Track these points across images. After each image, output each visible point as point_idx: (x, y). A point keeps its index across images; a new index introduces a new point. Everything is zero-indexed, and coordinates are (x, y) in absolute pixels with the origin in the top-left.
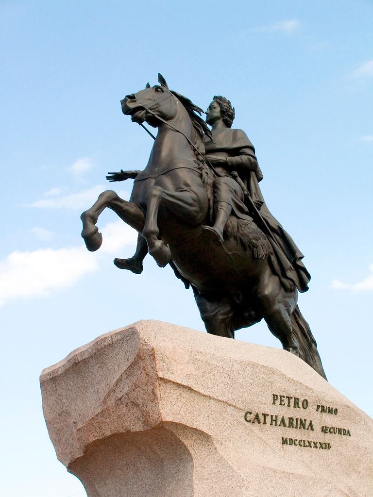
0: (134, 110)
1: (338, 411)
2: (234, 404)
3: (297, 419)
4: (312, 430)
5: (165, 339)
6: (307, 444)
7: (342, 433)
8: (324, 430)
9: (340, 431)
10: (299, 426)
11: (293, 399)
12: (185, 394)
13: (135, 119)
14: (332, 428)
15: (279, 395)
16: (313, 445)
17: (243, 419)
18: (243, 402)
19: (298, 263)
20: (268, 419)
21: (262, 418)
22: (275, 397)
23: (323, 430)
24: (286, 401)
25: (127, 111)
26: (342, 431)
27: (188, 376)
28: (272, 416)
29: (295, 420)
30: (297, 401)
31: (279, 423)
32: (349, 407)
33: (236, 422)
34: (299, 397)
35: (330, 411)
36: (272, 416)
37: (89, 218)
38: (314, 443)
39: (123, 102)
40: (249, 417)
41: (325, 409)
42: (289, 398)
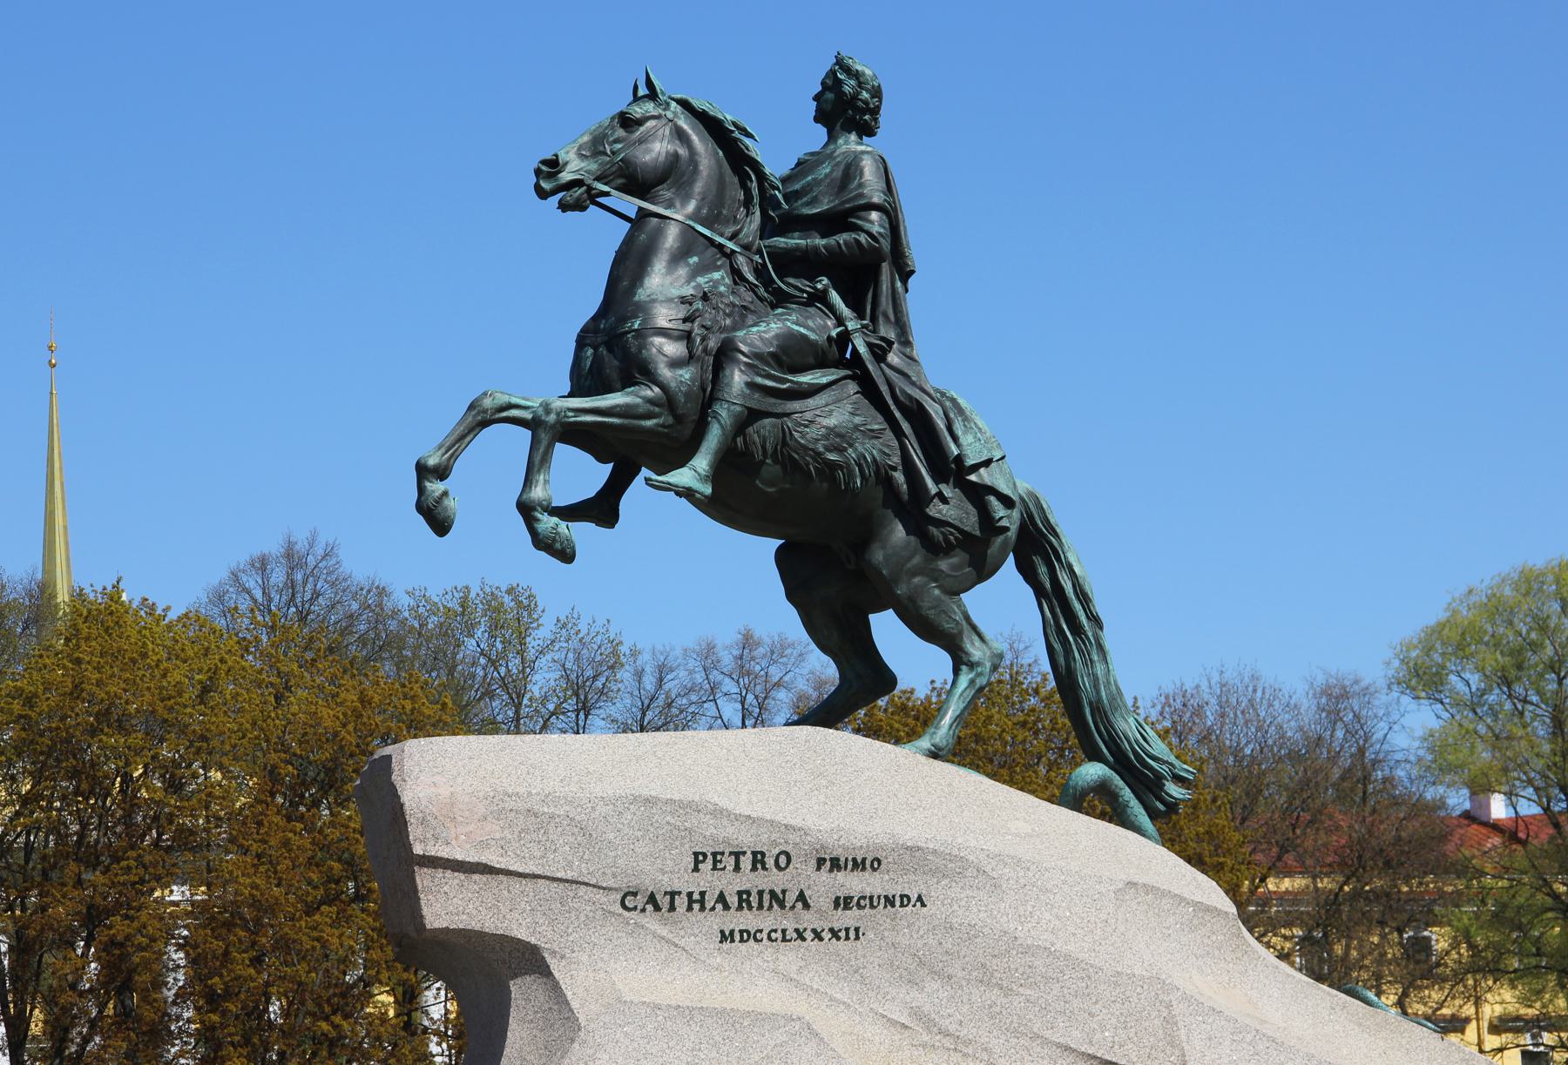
1: (884, 862)
2: (593, 881)
3: (761, 893)
4: (806, 906)
5: (437, 778)
6: (791, 934)
7: (898, 903)
8: (842, 903)
9: (890, 901)
10: (766, 904)
11: (749, 855)
12: (476, 877)
13: (564, 207)
14: (864, 898)
15: (709, 850)
16: (809, 935)
17: (618, 905)
18: (614, 876)
19: (973, 478)
20: (681, 902)
21: (664, 902)
24: (732, 860)
25: (542, 194)
26: (898, 899)
27: (484, 845)
28: (690, 895)
30: (758, 860)
31: (709, 905)
32: (919, 849)
33: (600, 912)
34: (764, 849)
35: (859, 865)
38: (814, 931)
39: (538, 172)
40: (629, 902)
41: (842, 863)
42: (737, 855)
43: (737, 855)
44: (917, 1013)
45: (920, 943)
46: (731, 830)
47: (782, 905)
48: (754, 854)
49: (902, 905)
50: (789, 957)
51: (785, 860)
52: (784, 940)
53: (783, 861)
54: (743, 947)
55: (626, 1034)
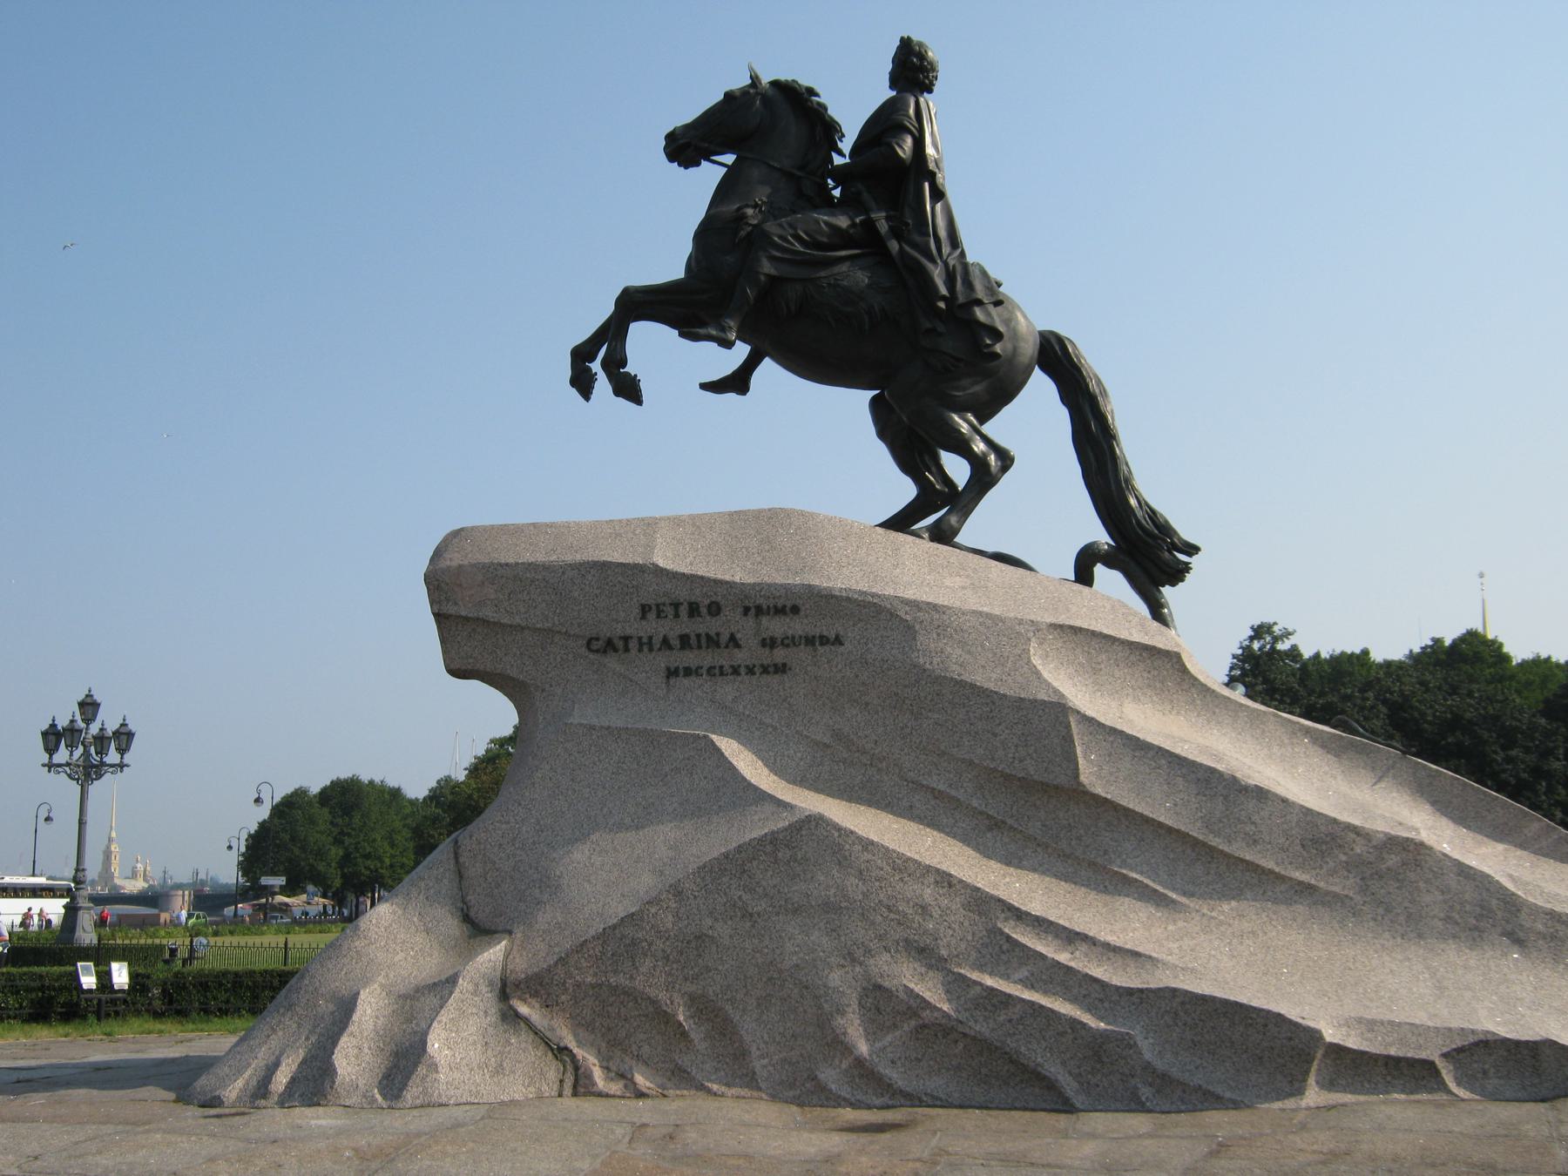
0: (685, 147)
3: (698, 636)
4: (738, 646)
9: (810, 641)
16: (743, 670)
20: (633, 644)
21: (620, 644)
22: (645, 610)
23: (763, 643)
24: (670, 611)
29: (693, 637)
30: (694, 610)
32: (833, 596)
35: (780, 611)
36: (640, 638)
37: (581, 355)
40: (595, 645)
42: (676, 606)
43: (676, 606)
44: (837, 735)
45: (839, 676)
46: (668, 586)
47: (718, 646)
48: (690, 604)
49: (822, 644)
50: (727, 689)
51: (715, 609)
52: (722, 674)
53: (714, 608)
54: (686, 681)
55: (566, 750)
